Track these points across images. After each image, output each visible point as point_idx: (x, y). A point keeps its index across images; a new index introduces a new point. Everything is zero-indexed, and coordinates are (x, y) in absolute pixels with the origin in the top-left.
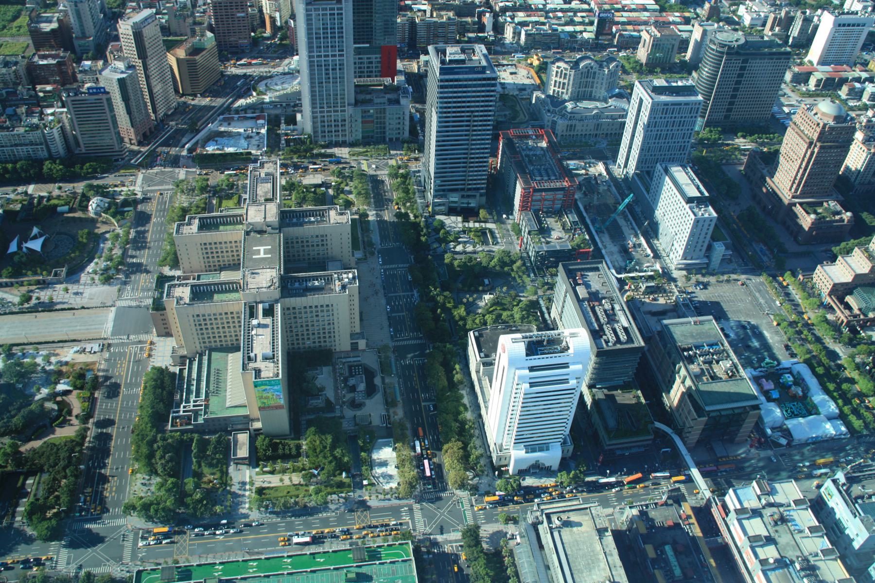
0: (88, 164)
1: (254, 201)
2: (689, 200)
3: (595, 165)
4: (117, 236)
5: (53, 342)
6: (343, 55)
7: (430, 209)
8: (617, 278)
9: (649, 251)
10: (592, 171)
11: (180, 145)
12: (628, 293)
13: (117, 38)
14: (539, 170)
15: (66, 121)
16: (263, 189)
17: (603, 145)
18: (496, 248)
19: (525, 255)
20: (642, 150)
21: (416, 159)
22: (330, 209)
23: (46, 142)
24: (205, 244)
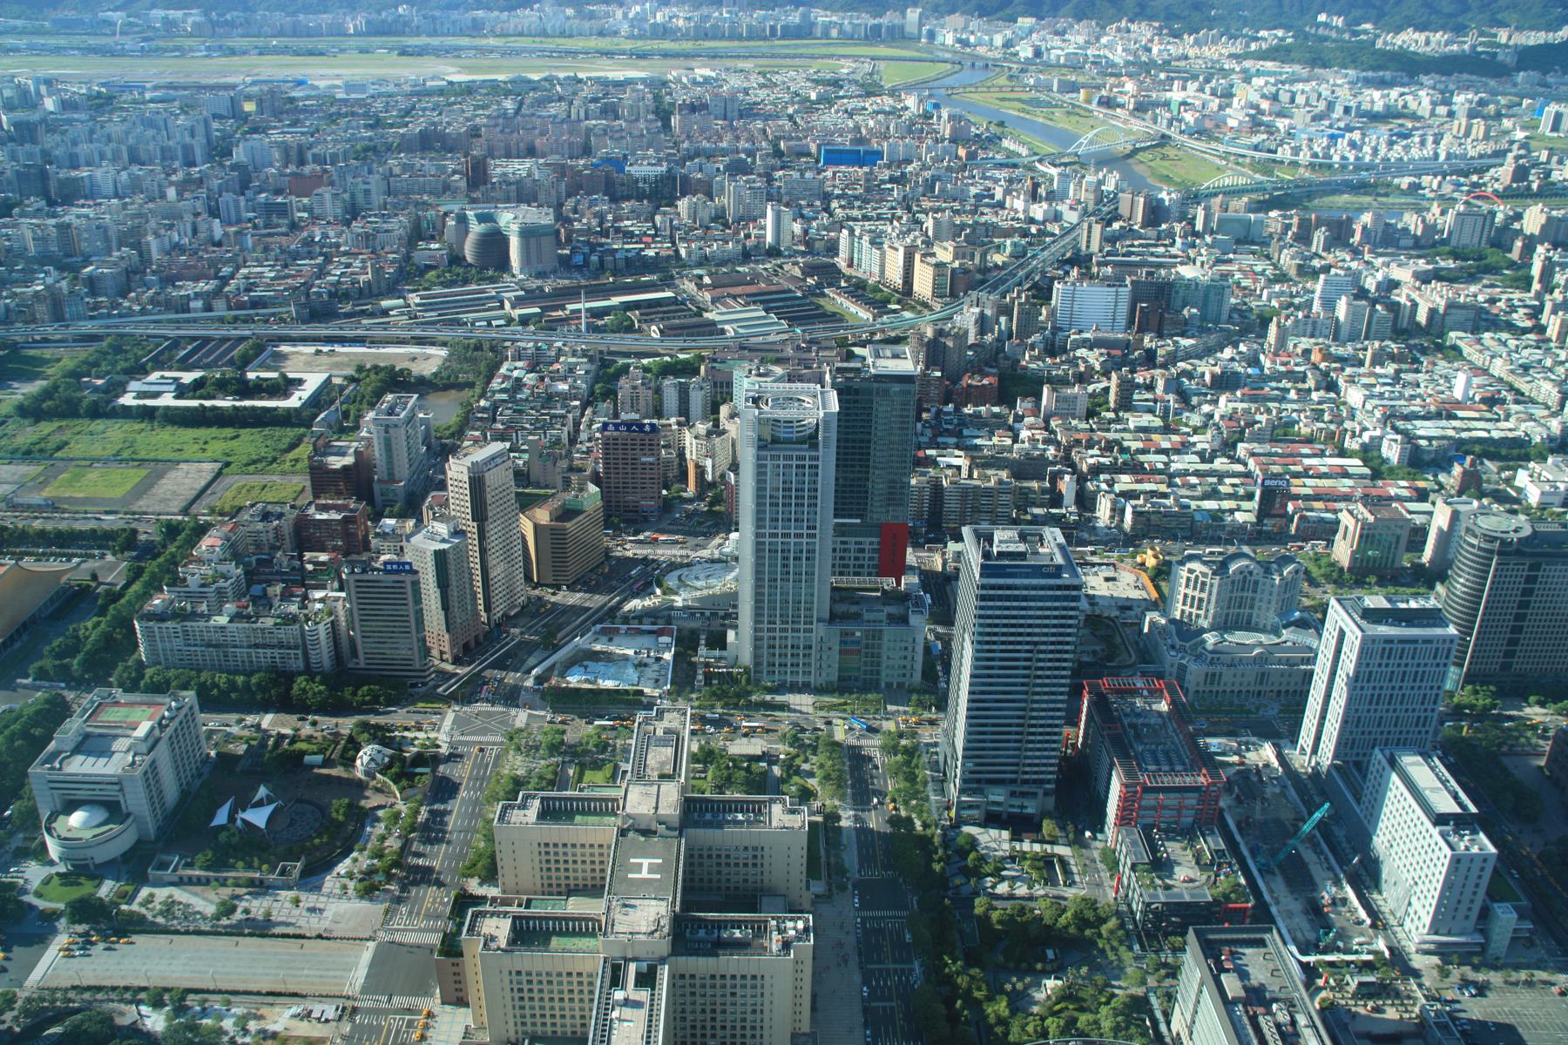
0: (365, 688)
1: (640, 776)
2: (1440, 820)
3: (1257, 747)
4: (397, 816)
5: (259, 993)
6: (814, 536)
7: (953, 814)
8: (1300, 962)
9: (1362, 914)
10: (1252, 757)
11: (524, 668)
12: (1323, 994)
13: (442, 485)
14: (1153, 753)
15: (341, 613)
16: (659, 757)
17: (1272, 711)
18: (1070, 893)
19: (1124, 908)
20: (1345, 722)
21: (932, 723)
22: (772, 801)
23: (304, 645)
24: (547, 845)
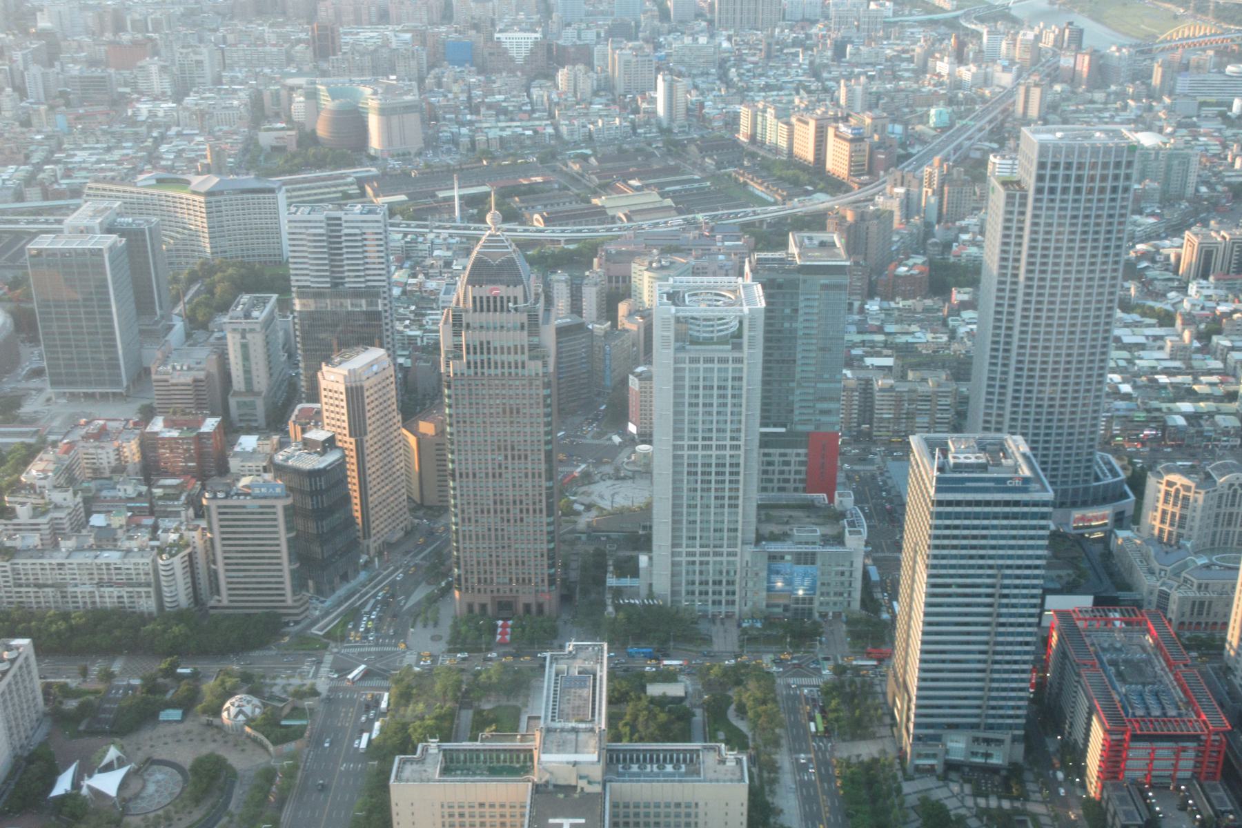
6: (737, 447)
13: (314, 396)
